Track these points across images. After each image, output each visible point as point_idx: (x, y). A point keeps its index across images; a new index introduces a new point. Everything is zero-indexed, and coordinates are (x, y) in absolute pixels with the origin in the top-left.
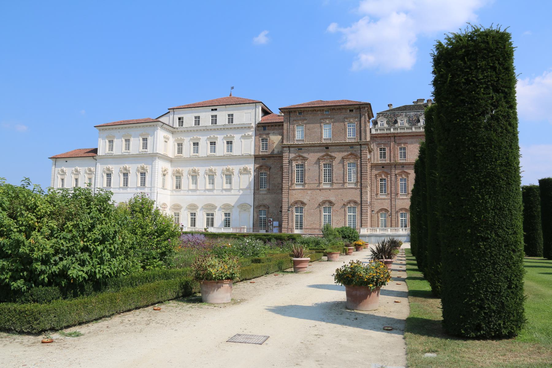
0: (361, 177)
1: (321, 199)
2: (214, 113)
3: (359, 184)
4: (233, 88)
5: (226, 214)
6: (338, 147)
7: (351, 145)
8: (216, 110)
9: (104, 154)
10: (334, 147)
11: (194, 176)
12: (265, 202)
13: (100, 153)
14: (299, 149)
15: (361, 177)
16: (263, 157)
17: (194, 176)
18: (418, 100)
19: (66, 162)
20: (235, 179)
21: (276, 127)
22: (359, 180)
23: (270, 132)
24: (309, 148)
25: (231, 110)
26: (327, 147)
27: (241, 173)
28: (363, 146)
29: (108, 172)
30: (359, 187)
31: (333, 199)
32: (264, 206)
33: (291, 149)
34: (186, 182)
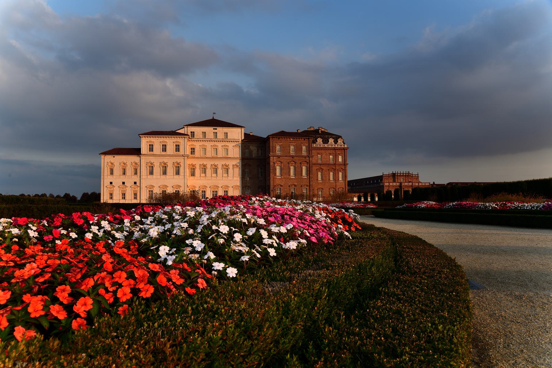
0: (309, 173)
2: (215, 131)
4: (214, 113)
5: (225, 191)
7: (305, 157)
8: (216, 129)
9: (147, 153)
11: (204, 169)
14: (278, 158)
15: (309, 173)
16: (247, 159)
17: (204, 169)
19: (114, 157)
20: (231, 171)
21: (254, 143)
22: (309, 175)
23: (250, 145)
24: (284, 158)
25: (226, 130)
26: (293, 157)
30: (308, 178)
31: (296, 184)
33: (275, 157)
34: (198, 172)
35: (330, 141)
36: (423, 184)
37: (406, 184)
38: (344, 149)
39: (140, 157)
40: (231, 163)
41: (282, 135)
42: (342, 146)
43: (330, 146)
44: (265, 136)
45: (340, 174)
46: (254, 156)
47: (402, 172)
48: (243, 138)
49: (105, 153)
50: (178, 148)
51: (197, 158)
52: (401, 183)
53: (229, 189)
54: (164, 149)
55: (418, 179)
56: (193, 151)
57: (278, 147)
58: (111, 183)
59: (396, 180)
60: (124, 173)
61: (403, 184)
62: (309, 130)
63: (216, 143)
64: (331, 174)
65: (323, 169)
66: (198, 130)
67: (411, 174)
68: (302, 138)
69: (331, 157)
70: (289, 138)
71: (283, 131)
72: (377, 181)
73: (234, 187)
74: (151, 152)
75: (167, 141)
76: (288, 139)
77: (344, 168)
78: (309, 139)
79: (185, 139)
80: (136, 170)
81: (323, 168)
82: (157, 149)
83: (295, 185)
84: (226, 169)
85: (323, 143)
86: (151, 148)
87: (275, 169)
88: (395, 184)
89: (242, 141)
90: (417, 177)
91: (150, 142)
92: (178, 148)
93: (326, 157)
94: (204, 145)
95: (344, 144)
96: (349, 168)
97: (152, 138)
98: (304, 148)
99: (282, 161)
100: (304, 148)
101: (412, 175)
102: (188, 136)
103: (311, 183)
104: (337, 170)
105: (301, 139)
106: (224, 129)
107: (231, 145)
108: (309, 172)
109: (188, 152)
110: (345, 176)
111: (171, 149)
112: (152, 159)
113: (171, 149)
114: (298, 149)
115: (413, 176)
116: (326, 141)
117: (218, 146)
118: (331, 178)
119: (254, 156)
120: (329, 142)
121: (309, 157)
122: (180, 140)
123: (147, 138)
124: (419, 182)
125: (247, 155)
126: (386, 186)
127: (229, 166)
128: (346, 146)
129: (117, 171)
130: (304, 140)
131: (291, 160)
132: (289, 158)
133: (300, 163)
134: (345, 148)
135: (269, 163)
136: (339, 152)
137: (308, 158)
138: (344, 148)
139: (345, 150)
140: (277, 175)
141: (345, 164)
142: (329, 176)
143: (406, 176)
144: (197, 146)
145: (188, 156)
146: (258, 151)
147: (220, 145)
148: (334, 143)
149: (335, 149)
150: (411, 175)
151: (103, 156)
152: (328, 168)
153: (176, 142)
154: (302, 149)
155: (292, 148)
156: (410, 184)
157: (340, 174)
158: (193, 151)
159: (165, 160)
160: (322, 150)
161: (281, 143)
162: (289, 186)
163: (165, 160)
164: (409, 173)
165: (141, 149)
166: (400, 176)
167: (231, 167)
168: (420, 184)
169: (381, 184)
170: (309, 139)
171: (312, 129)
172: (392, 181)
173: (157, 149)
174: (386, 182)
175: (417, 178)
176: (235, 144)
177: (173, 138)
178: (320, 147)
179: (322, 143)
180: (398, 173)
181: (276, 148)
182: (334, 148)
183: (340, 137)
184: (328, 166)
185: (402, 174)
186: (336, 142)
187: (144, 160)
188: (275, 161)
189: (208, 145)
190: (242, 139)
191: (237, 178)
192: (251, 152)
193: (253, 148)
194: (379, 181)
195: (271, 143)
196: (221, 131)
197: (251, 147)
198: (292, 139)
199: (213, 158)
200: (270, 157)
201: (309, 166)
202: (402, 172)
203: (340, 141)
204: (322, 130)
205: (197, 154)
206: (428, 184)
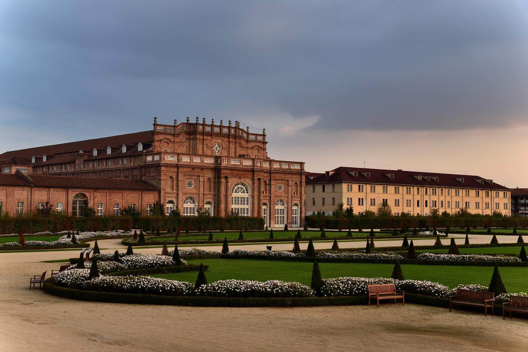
37: (234, 162)
52: (217, 158)
55: (264, 149)
59: (199, 147)
61: (225, 163)
67: (243, 131)
72: (132, 147)
88: (197, 160)
101: (248, 134)
115: (252, 137)
126: (167, 165)
143: (228, 136)
150: (245, 135)
156: (247, 163)
164: (237, 128)
166: (211, 134)
169: (149, 158)
172: (183, 149)
174: (166, 153)
175: (261, 145)
180: (204, 125)
185: (217, 130)
194: (140, 148)
202: (209, 122)
206: (298, 167)
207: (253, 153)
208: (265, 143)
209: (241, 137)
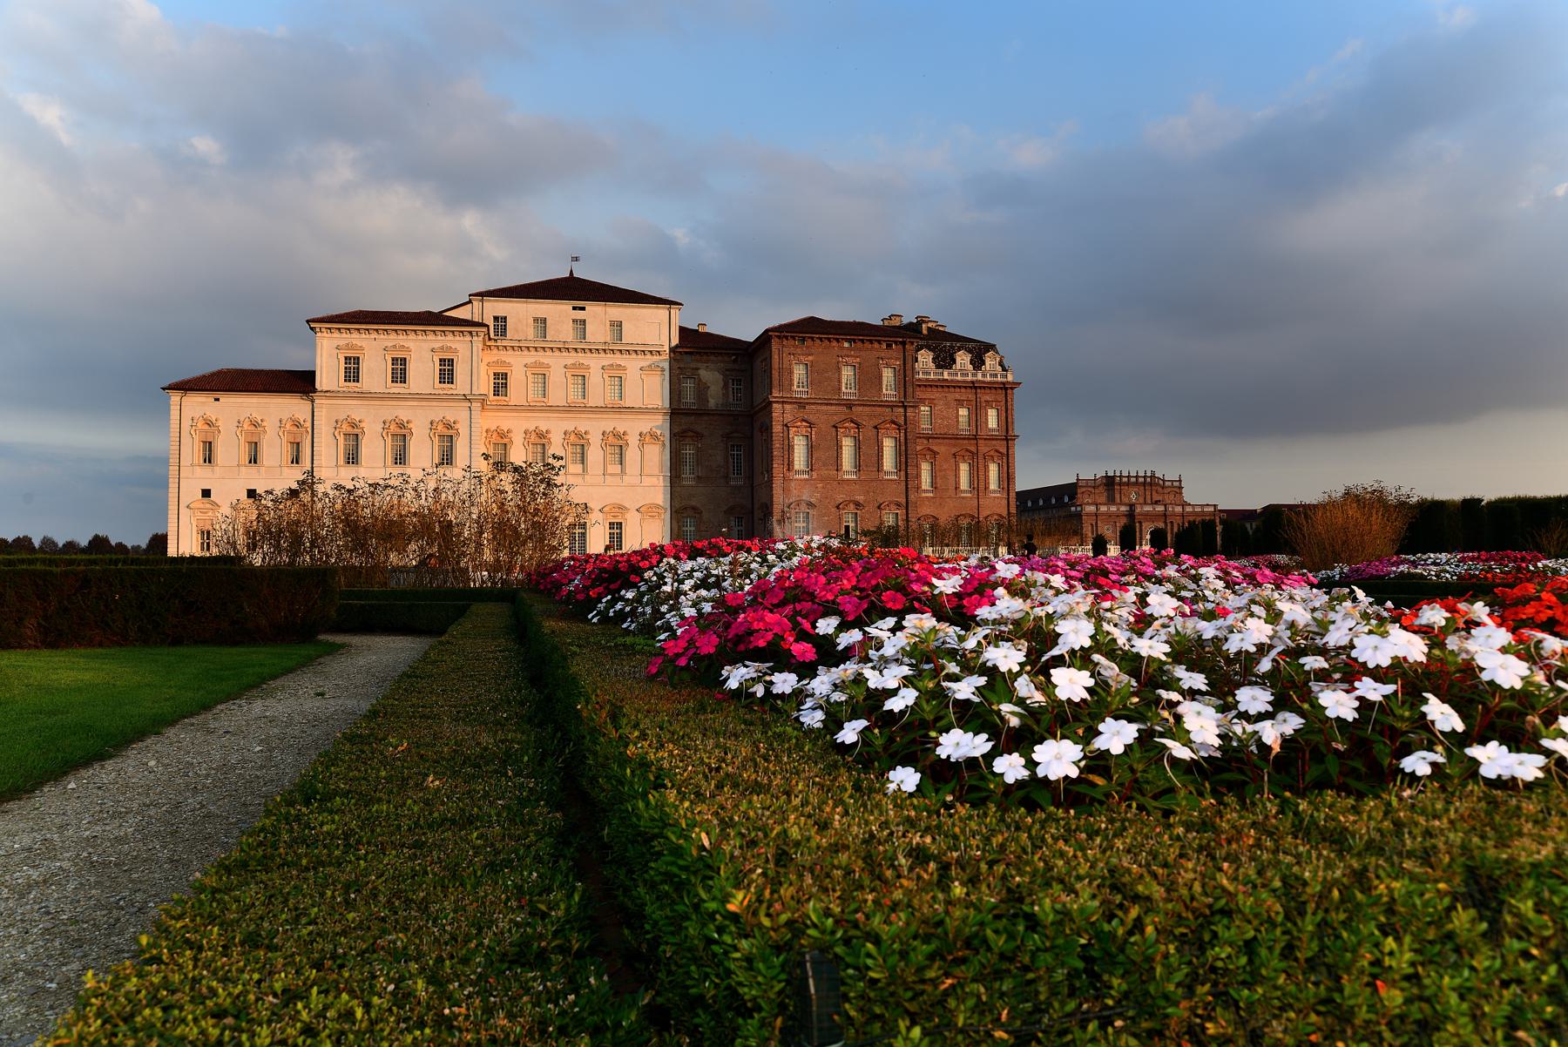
1: (840, 498)
2: (580, 315)
3: (903, 473)
4: (576, 259)
6: (867, 409)
7: (892, 407)
8: (583, 309)
9: (335, 388)
10: (861, 408)
12: (693, 503)
13: (322, 382)
16: (688, 413)
18: (921, 320)
19: (217, 400)
20: (632, 454)
21: (712, 358)
22: (903, 467)
23: (699, 365)
24: (819, 407)
25: (616, 311)
26: (849, 405)
27: (642, 443)
28: (909, 410)
29: (350, 430)
30: (903, 478)
31: (860, 498)
32: (694, 508)
33: (787, 407)
35: (958, 360)
36: (1198, 509)
37: (1148, 508)
38: (1006, 388)
39: (313, 402)
40: (633, 427)
41: (809, 329)
42: (996, 376)
43: (959, 378)
44: (749, 334)
45: (993, 470)
46: (712, 403)
47: (1125, 474)
48: (675, 341)
49: (186, 387)
50: (447, 372)
51: (517, 408)
52: (1132, 506)
53: (628, 516)
54: (400, 371)
56: (501, 383)
57: (799, 372)
58: (206, 493)
59: (1117, 496)
60: (254, 460)
61: (1138, 510)
62: (886, 323)
63: (581, 358)
64: (964, 468)
65: (935, 453)
66: (520, 312)
68: (879, 342)
69: (963, 412)
70: (838, 340)
71: (812, 318)
72: (1060, 499)
73: (645, 511)
74: (352, 384)
75: (411, 345)
76: (834, 344)
77: (1004, 451)
78: (904, 344)
79: (475, 338)
80: (297, 446)
81: (935, 448)
82: (375, 373)
83: (858, 505)
84: (617, 446)
85: (938, 367)
86: (352, 370)
87: (790, 448)
88: (1113, 508)
89: (672, 350)
90: (1178, 488)
91: (349, 347)
92: (447, 372)
93: (945, 413)
94: (541, 365)
95: (1004, 369)
96: (1020, 454)
97: (355, 335)
98: (888, 375)
99: (812, 418)
100: (888, 375)
102: (485, 329)
103: (912, 497)
104: (981, 456)
105: (876, 345)
106: (608, 309)
107: (633, 365)
108: (903, 460)
109: (485, 385)
110: (1007, 477)
111: (422, 374)
112: (357, 411)
113: (422, 374)
114: (869, 379)
116: (945, 360)
117: (588, 368)
118: (964, 483)
119: (712, 403)
120: (955, 362)
121: (905, 407)
122: (459, 345)
123: (336, 334)
124: (1184, 504)
125: (689, 398)
126: (1088, 514)
127: (626, 437)
128: (1010, 378)
129: (229, 449)
130: (889, 346)
131: (844, 417)
132: (838, 408)
133: (875, 427)
134: (1009, 383)
135: (767, 429)
136: (988, 398)
137: (902, 410)
138: (1004, 383)
139: (1006, 389)
140: (797, 467)
141: (1007, 437)
142: (957, 476)
143: (1144, 484)
144: (517, 365)
145: (483, 401)
146: (726, 386)
147: (595, 363)
148: (971, 367)
149: (973, 386)
151: (175, 397)
152: (954, 450)
153: (442, 348)
154: (880, 377)
155: (847, 374)
156: (1160, 508)
157: (993, 470)
158: (501, 383)
159: (403, 412)
160: (935, 390)
161: (810, 358)
162: (838, 507)
163: (403, 412)
164: (1153, 476)
165: (314, 372)
166: (1128, 484)
167: (633, 440)
168: (1189, 509)
169: (1073, 509)
170: (904, 344)
171: (896, 322)
172: (1103, 499)
173: (375, 373)
174: (1088, 504)
176: (648, 363)
177: (431, 337)
178: (927, 380)
179: (932, 365)
181: (791, 372)
182: (973, 382)
183: (989, 347)
184: (953, 441)
185: (1133, 480)
186: (978, 363)
187: (327, 413)
188: (788, 417)
189: (556, 364)
190: (673, 344)
191: (654, 480)
192: (702, 390)
193: (711, 375)
194: (1066, 499)
195: (775, 357)
196: (598, 315)
197: (702, 372)
198: (846, 345)
199: (570, 409)
200: (771, 403)
201: (906, 439)
202: (1125, 474)
203: (990, 361)
204: (930, 325)
205: (515, 394)
207: (1169, 499)
208: (1181, 488)
209: (1158, 484)
